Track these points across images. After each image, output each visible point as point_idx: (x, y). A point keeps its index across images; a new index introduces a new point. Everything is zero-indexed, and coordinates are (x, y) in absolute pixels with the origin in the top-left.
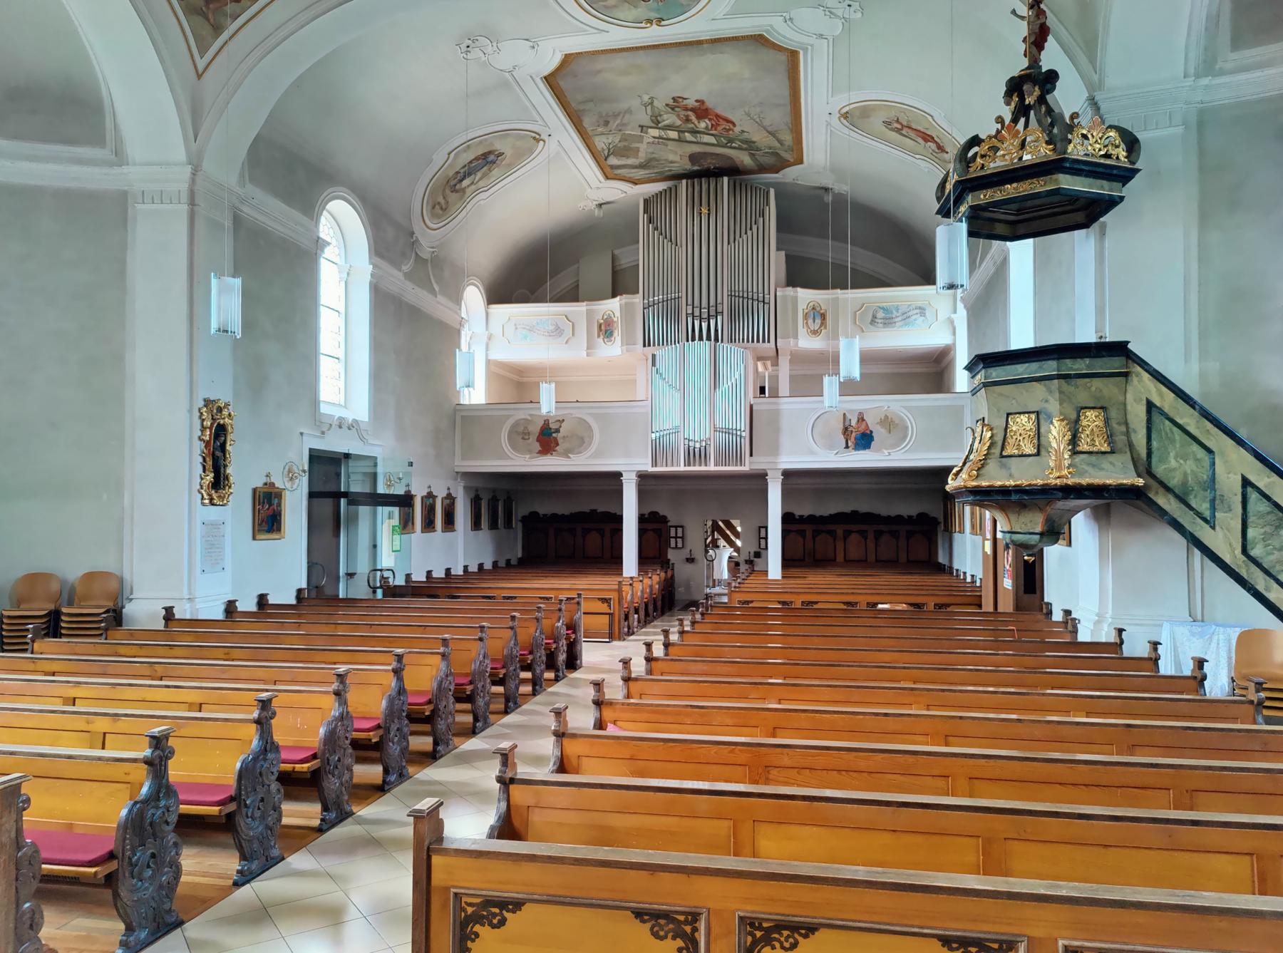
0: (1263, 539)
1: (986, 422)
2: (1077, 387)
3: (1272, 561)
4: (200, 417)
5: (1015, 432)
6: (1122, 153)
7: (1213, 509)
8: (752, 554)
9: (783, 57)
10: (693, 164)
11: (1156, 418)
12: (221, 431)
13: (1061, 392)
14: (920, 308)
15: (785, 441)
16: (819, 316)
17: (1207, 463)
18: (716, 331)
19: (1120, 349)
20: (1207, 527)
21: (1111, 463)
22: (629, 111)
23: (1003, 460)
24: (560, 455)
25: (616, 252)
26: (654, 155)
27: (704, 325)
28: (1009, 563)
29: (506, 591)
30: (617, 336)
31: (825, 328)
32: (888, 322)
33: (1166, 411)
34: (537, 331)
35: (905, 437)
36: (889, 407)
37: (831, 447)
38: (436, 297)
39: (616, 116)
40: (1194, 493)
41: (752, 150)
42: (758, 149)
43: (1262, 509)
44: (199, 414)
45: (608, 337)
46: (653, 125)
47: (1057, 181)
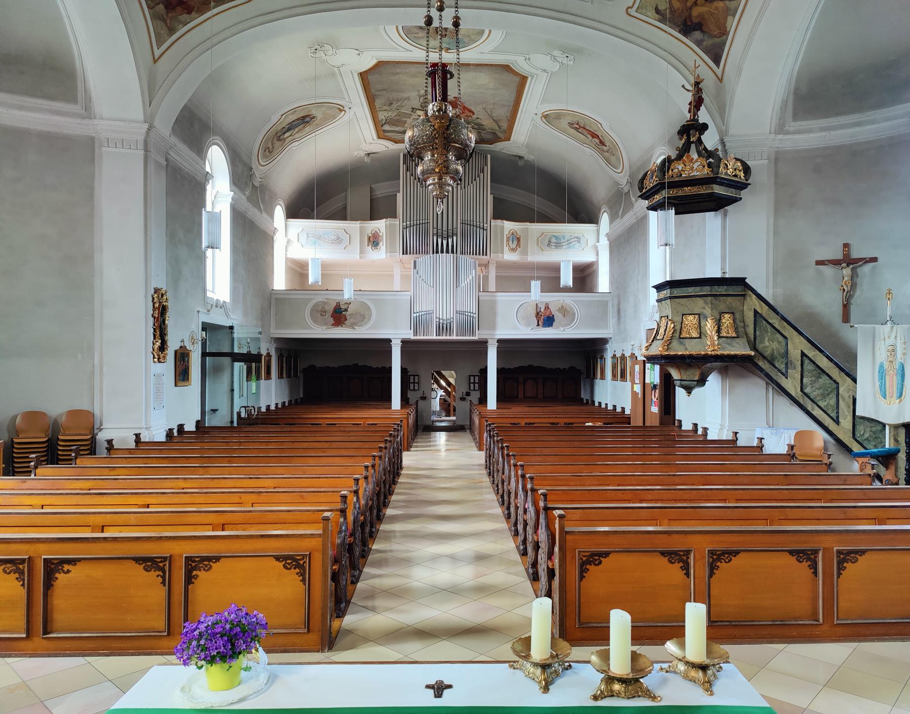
0: (811, 384)
1: (670, 318)
2: (720, 301)
3: (815, 395)
4: (153, 301)
5: (687, 325)
6: (742, 175)
7: (787, 368)
8: (465, 393)
9: (517, 79)
11: (759, 319)
12: (163, 310)
13: (711, 304)
14: (577, 238)
15: (500, 320)
16: (517, 240)
17: (784, 344)
18: (453, 246)
19: (740, 282)
20: (784, 377)
21: (738, 343)
22: (408, 99)
23: (681, 340)
24: (348, 327)
25: (373, 186)
27: (445, 242)
28: (656, 397)
29: (328, 420)
30: (383, 246)
31: (520, 247)
32: (558, 245)
33: (764, 316)
34: (323, 239)
35: (573, 320)
36: (564, 300)
37: (528, 325)
38: (262, 213)
39: (398, 100)
40: (777, 359)
42: (484, 130)
43: (810, 368)
44: (152, 299)
45: (375, 246)
46: (421, 108)
47: (712, 188)
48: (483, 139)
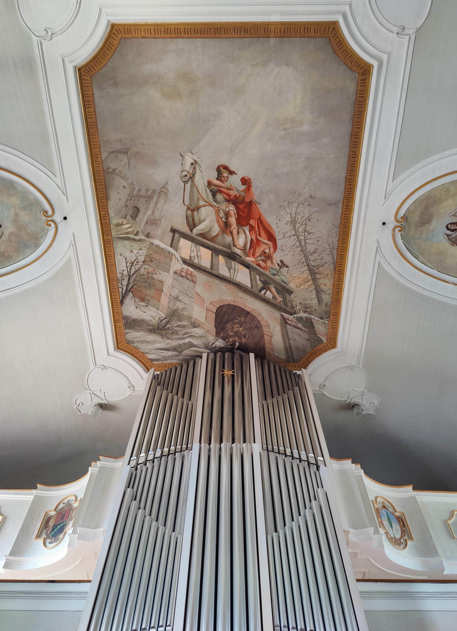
10: (217, 334)
26: (179, 305)
48: (290, 346)
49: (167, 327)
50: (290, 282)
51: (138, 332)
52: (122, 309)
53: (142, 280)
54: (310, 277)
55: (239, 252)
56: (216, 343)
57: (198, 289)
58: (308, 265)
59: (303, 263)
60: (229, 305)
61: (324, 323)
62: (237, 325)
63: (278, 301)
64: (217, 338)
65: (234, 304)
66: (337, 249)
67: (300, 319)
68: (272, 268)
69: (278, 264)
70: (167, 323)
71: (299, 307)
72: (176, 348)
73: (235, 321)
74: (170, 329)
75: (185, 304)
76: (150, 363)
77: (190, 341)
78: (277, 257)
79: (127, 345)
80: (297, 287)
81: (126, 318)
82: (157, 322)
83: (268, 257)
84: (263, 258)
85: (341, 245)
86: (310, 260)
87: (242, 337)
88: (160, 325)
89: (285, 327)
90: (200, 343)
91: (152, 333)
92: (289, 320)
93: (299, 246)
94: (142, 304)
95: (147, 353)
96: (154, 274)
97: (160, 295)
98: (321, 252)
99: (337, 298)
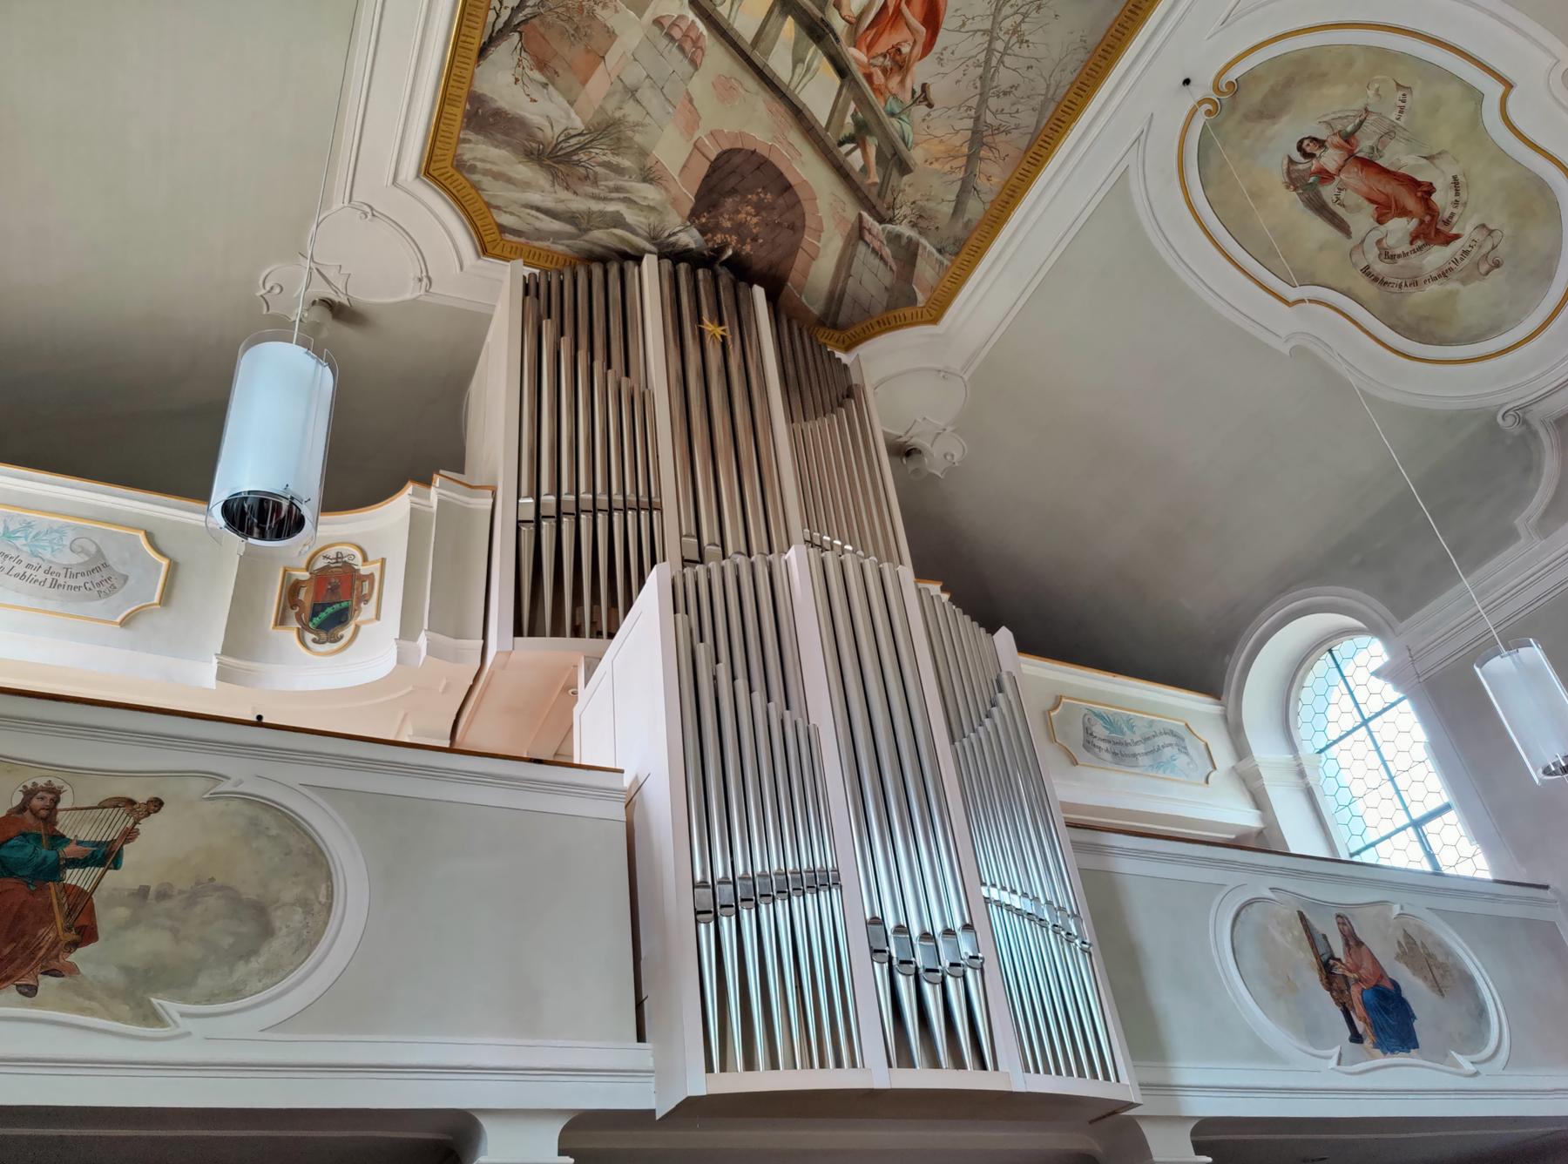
10: (694, 215)
26: (631, 112)
32: (1121, 753)
41: (872, 210)
49: (575, 158)
50: (917, 144)
51: (496, 147)
52: (476, 70)
53: (559, 10)
54: (965, 150)
55: (839, 25)
56: (680, 235)
57: (699, 87)
58: (977, 119)
59: (970, 108)
60: (754, 152)
61: (941, 263)
62: (749, 208)
63: (870, 181)
64: (689, 224)
65: (766, 155)
66: (1059, 104)
67: (895, 239)
68: (895, 96)
69: (914, 92)
70: (581, 148)
71: (905, 210)
72: (578, 217)
73: (750, 196)
74: (583, 166)
75: (648, 113)
76: (496, 236)
77: (618, 212)
78: (921, 72)
79: (452, 171)
80: (926, 161)
81: (476, 99)
82: (555, 137)
83: (899, 64)
84: (888, 63)
85: (1072, 96)
86: (987, 107)
87: (749, 240)
88: (561, 149)
89: (855, 246)
90: (641, 223)
91: (532, 160)
92: (870, 233)
93: (983, 65)
94: (536, 75)
95: (498, 208)
96: (601, 5)
97: (592, 68)
98: (1022, 98)
99: (995, 217)
